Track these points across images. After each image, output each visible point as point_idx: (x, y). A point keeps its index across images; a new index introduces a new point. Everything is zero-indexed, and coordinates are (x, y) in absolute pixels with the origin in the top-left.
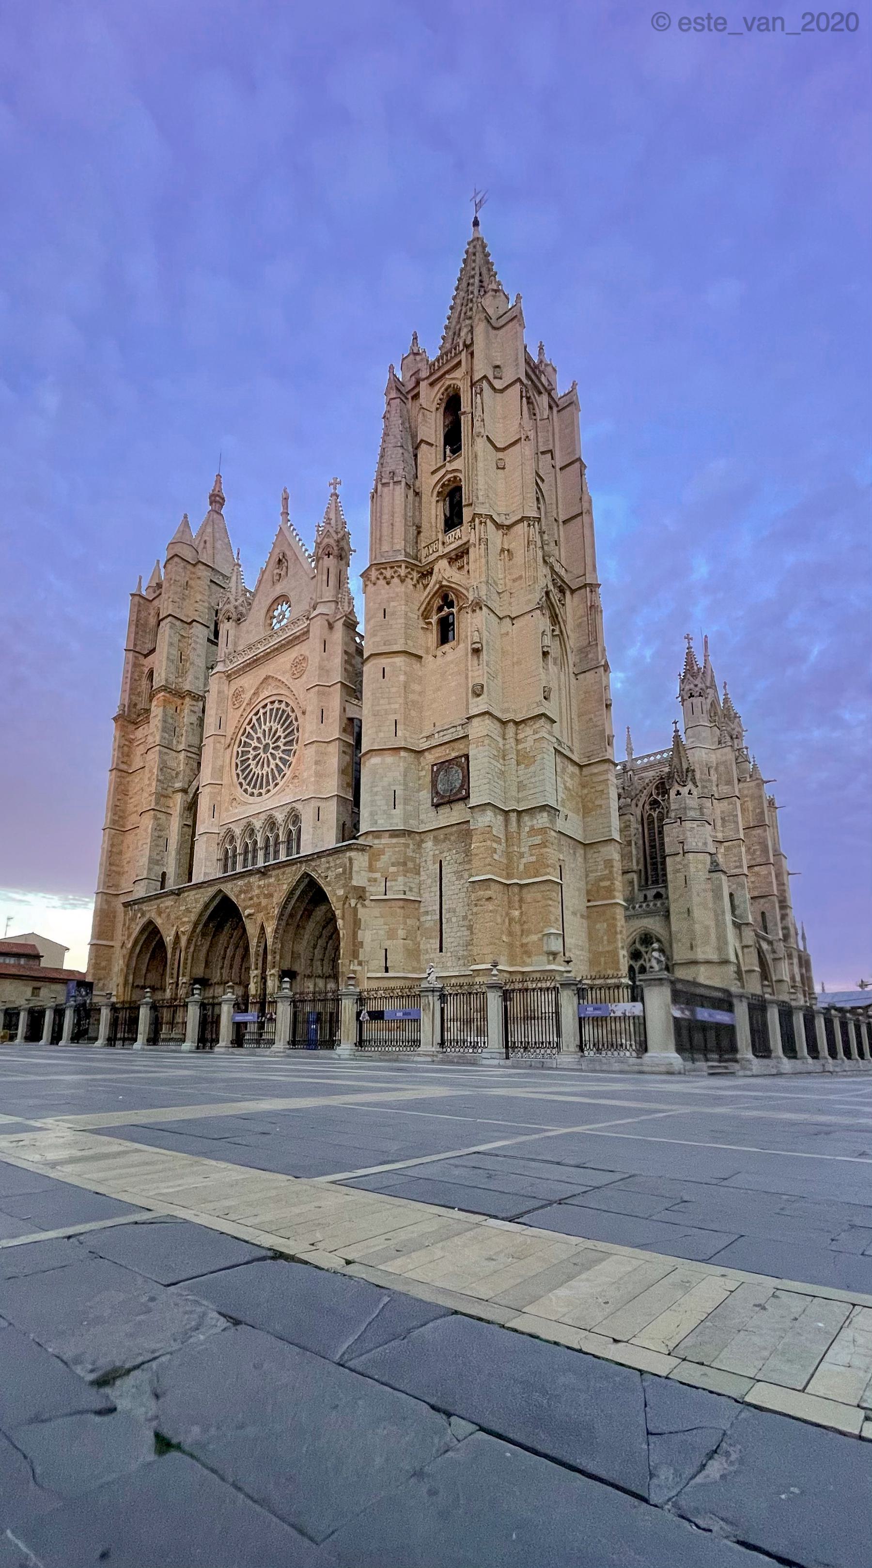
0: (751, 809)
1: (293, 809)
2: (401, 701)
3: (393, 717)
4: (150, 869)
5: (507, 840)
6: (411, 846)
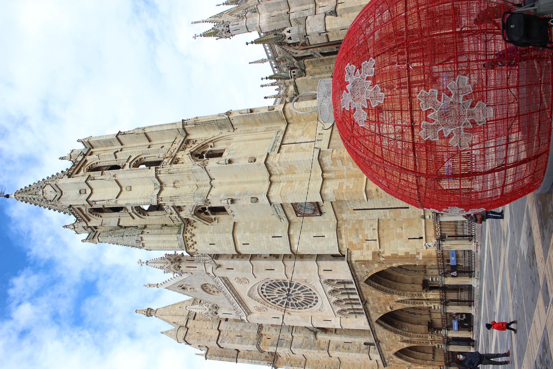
1: (325, 282)
6: (346, 226)
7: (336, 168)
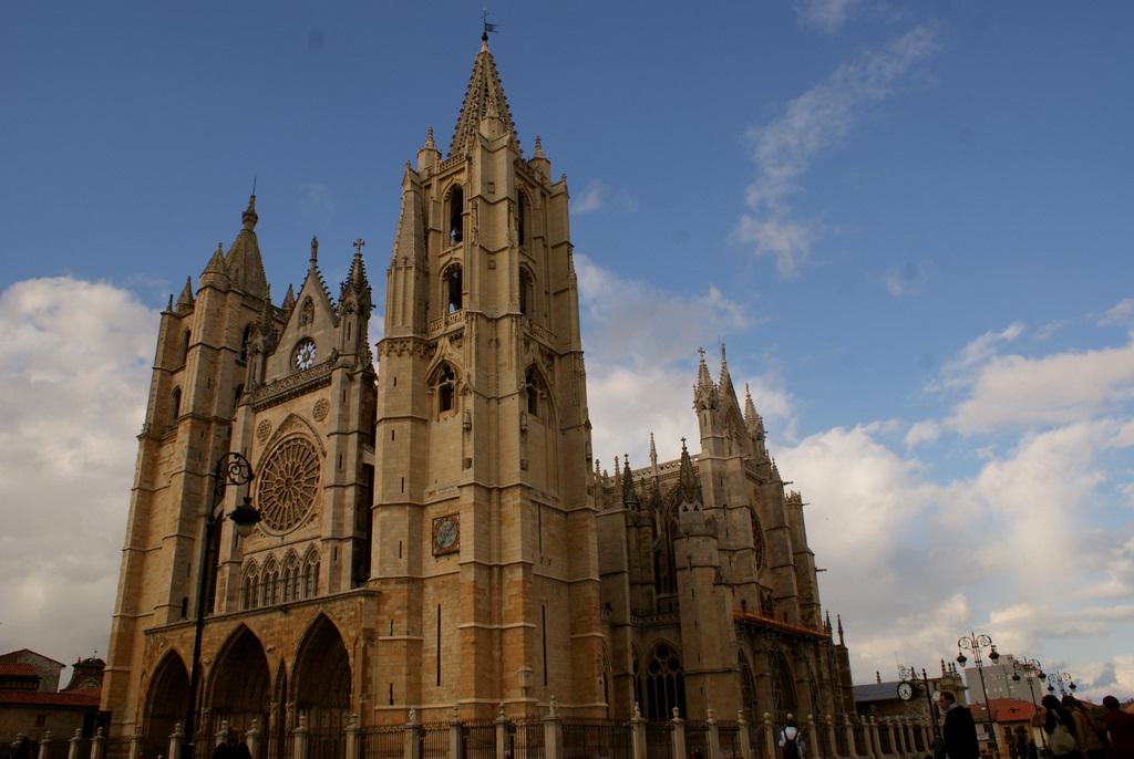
1: (312, 546)
2: (407, 460)
3: (401, 475)
5: (490, 592)
7: (505, 586)
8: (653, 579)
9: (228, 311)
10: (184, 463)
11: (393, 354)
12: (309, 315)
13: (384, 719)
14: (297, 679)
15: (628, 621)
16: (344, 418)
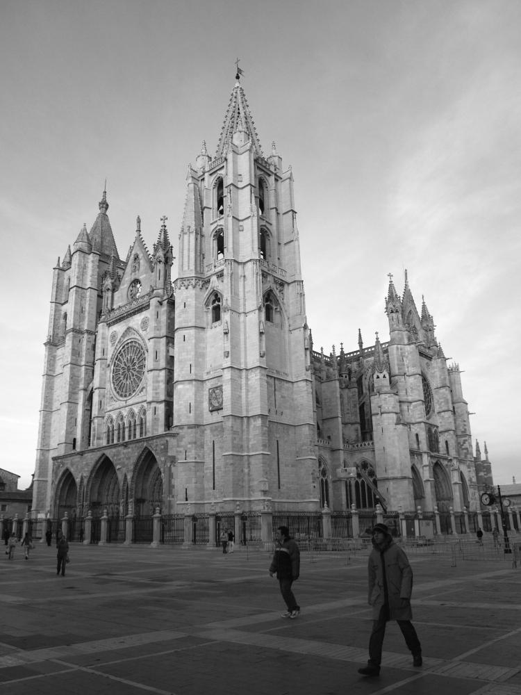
0: (438, 376)
1: (143, 406)
2: (193, 353)
3: (189, 363)
4: (66, 438)
8: (359, 421)
9: (90, 265)
10: (69, 360)
11: (183, 288)
12: (137, 266)
13: (183, 509)
14: (134, 486)
15: (342, 447)
16: (157, 328)
